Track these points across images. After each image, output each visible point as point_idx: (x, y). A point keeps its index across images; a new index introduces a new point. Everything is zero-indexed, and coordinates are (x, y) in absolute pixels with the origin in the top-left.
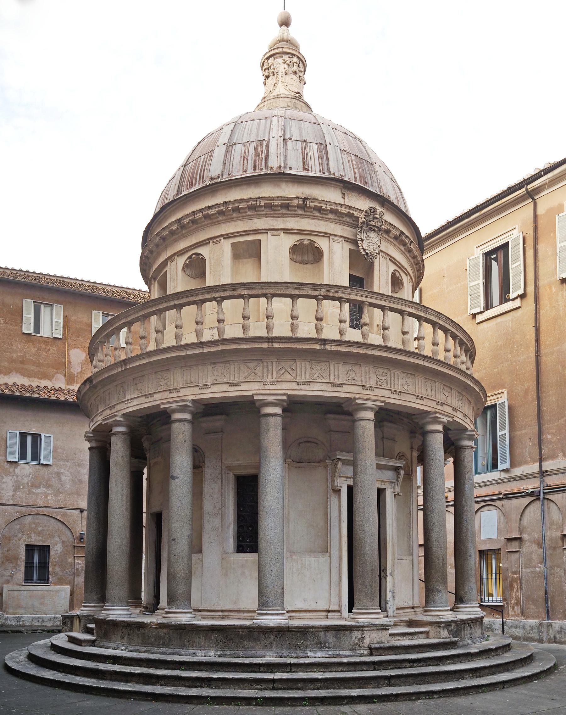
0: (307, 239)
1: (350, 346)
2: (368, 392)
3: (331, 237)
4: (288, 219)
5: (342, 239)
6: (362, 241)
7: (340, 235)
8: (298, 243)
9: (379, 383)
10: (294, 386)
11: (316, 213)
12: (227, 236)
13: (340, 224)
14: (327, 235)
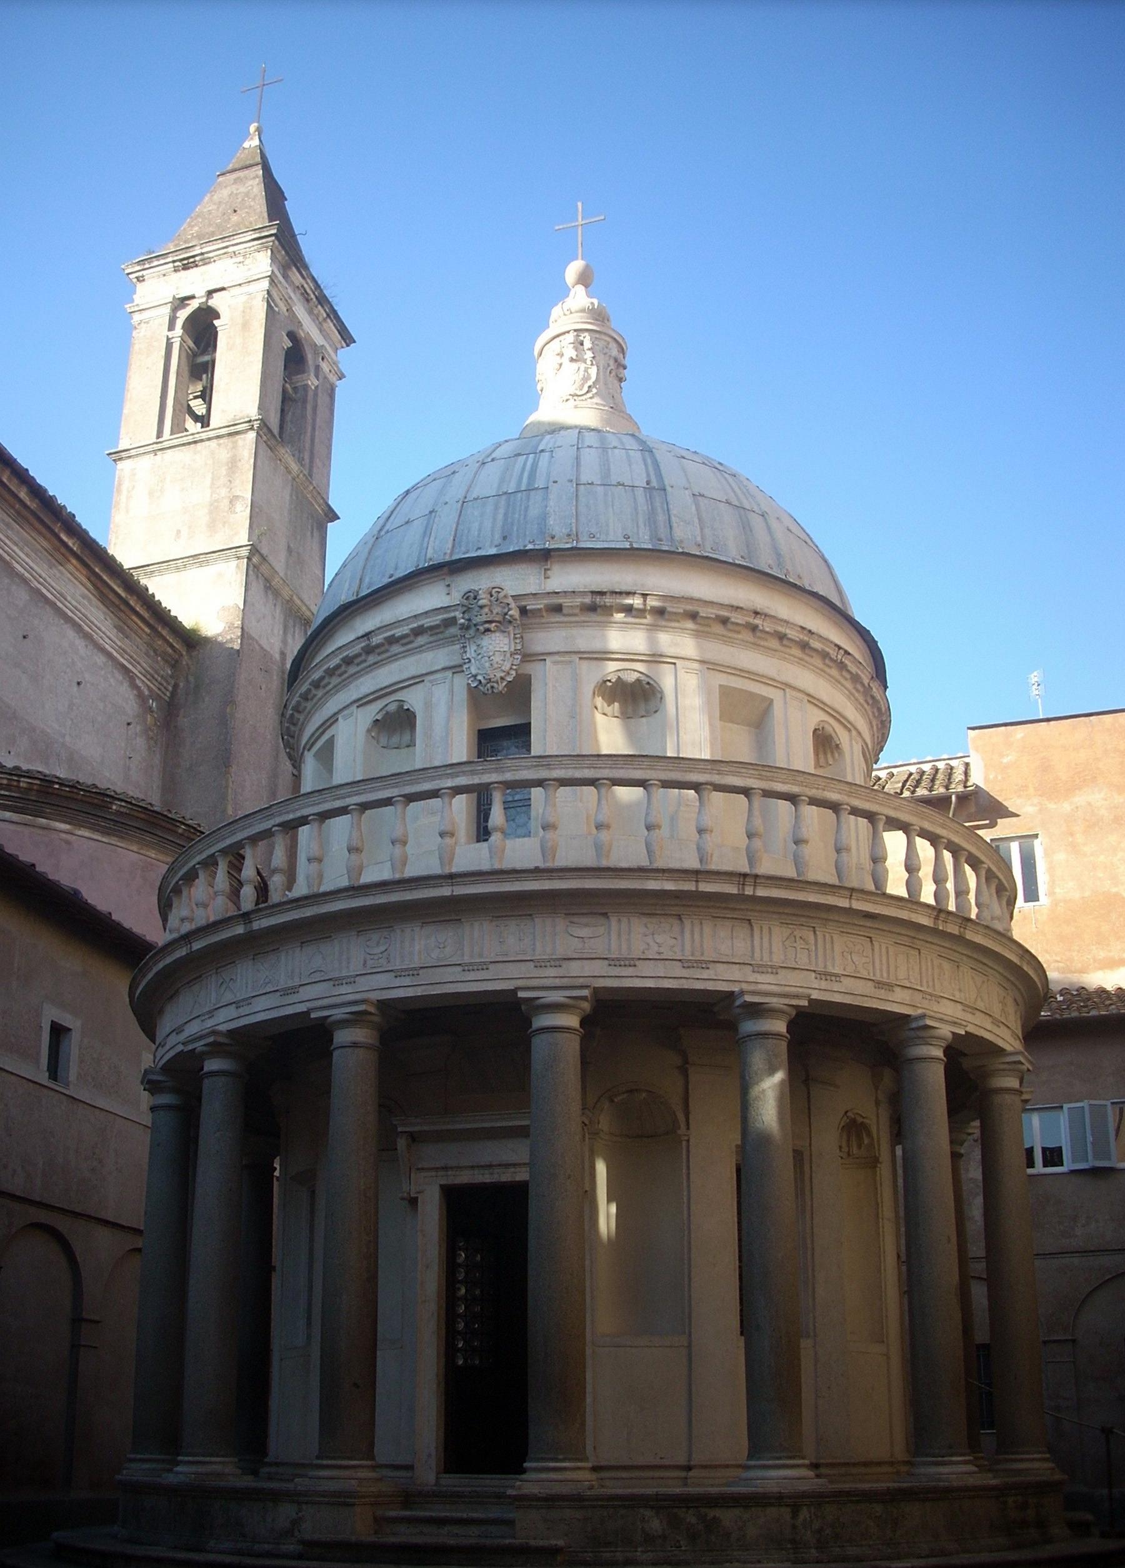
0: (390, 704)
1: (289, 910)
2: (344, 989)
3: (427, 678)
4: (361, 679)
5: (449, 674)
6: (470, 661)
7: (439, 667)
8: (379, 717)
9: (370, 963)
10: (232, 1012)
11: (396, 649)
12: (309, 746)
13: (443, 646)
14: (417, 680)
